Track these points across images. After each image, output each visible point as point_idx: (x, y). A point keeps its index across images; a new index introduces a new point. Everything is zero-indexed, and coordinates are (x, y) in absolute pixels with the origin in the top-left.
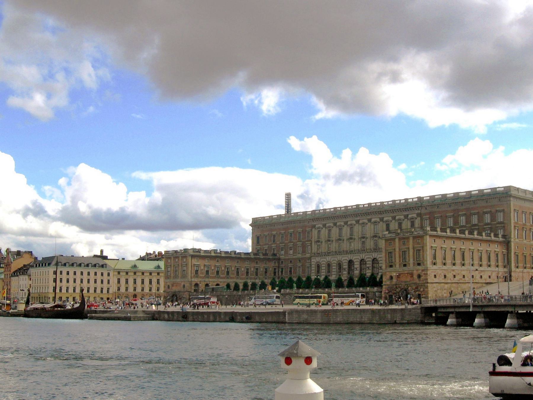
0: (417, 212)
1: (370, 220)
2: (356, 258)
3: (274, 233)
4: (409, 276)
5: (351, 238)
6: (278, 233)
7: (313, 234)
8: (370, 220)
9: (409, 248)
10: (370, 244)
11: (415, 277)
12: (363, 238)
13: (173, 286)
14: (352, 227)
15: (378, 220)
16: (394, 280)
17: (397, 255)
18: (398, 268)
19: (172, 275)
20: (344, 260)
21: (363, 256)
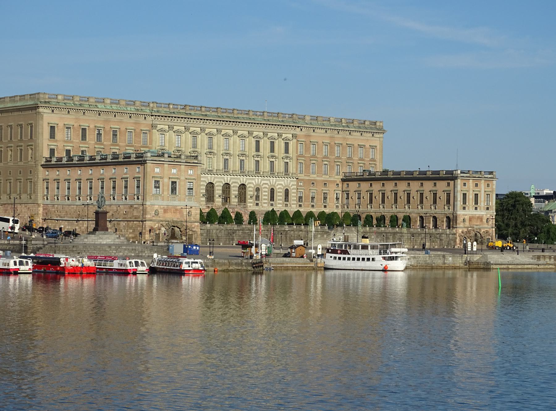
0: (292, 132)
1: (235, 132)
2: (219, 182)
3: (85, 124)
4: (479, 220)
6: (92, 126)
7: (154, 138)
8: (235, 132)
9: (480, 191)
10: (234, 164)
11: (485, 221)
12: (227, 154)
13: (165, 211)
14: (210, 136)
15: (246, 133)
16: (467, 224)
17: (471, 197)
18: (470, 212)
19: (165, 193)
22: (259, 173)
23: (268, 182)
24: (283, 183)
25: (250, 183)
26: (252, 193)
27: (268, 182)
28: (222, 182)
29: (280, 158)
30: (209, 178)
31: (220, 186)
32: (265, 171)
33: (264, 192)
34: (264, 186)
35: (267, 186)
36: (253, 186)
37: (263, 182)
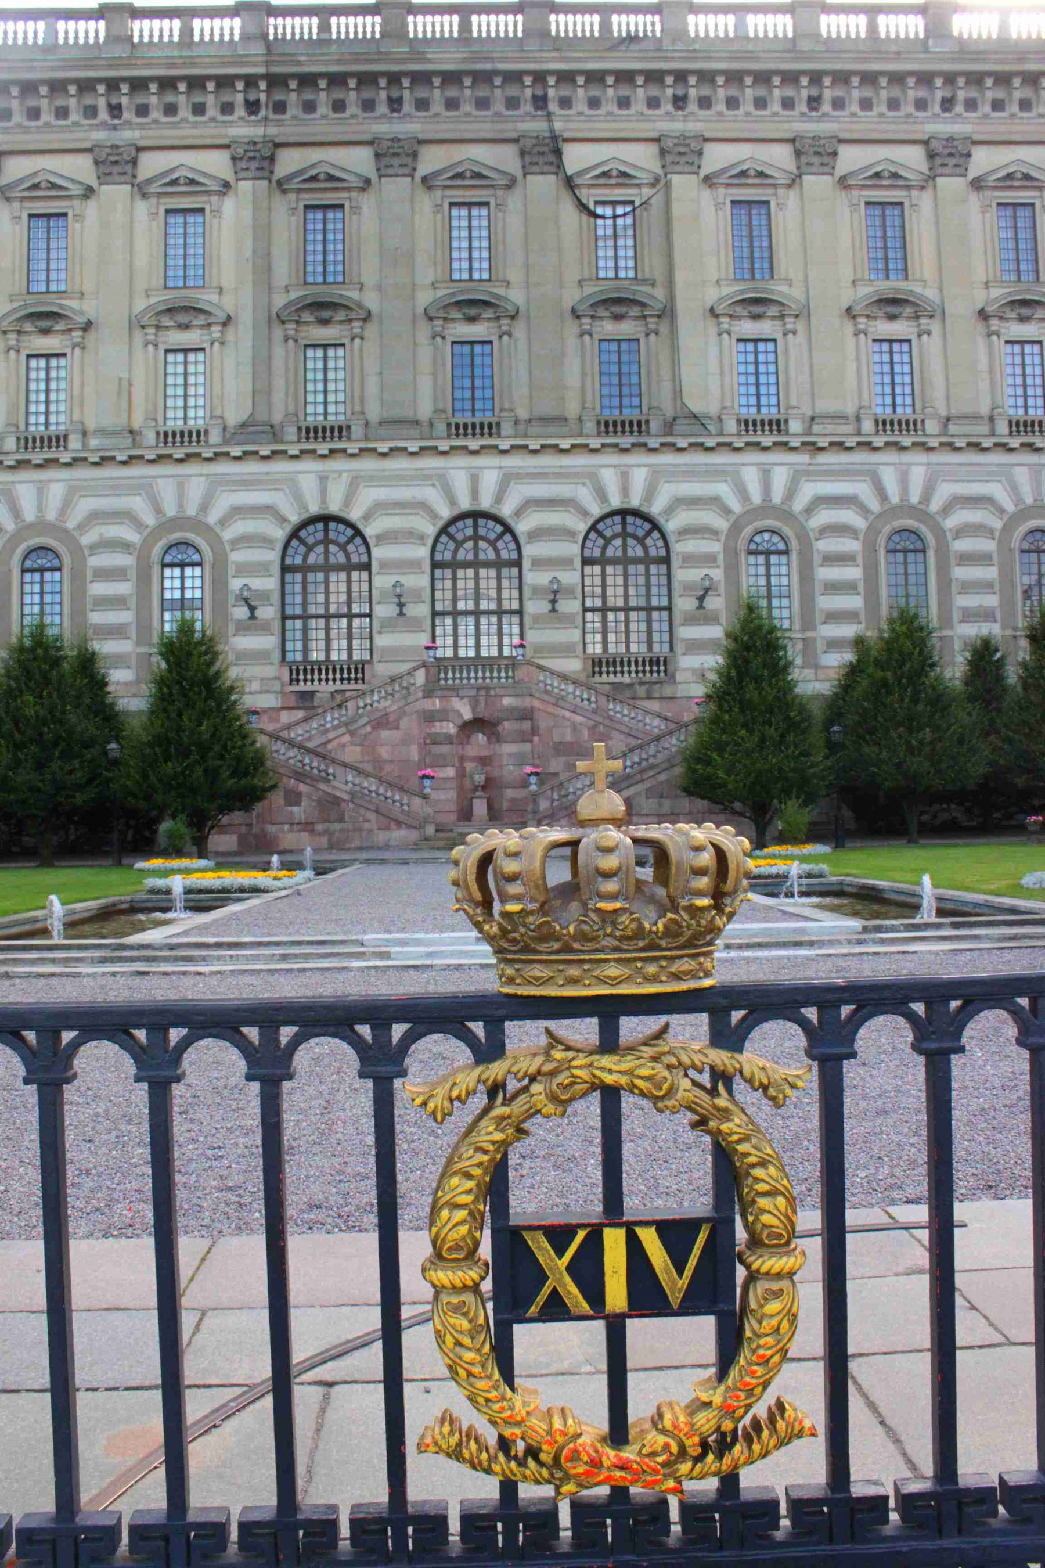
1: (546, 153)
5: (322, 308)
12: (473, 307)
20: (237, 512)
21: (476, 479)
22: (777, 425)
23: (862, 489)
24: (997, 490)
25: (694, 502)
26: (717, 574)
27: (862, 489)
28: (423, 507)
29: (962, 305)
30: (311, 484)
31: (413, 536)
32: (823, 406)
33: (831, 559)
34: (824, 517)
35: (848, 516)
36: (722, 524)
37: (808, 491)
